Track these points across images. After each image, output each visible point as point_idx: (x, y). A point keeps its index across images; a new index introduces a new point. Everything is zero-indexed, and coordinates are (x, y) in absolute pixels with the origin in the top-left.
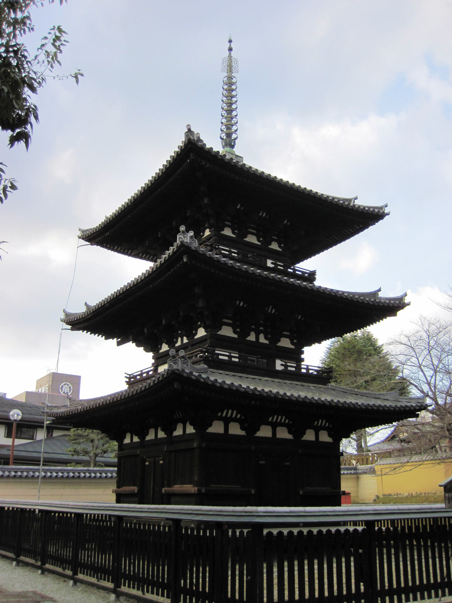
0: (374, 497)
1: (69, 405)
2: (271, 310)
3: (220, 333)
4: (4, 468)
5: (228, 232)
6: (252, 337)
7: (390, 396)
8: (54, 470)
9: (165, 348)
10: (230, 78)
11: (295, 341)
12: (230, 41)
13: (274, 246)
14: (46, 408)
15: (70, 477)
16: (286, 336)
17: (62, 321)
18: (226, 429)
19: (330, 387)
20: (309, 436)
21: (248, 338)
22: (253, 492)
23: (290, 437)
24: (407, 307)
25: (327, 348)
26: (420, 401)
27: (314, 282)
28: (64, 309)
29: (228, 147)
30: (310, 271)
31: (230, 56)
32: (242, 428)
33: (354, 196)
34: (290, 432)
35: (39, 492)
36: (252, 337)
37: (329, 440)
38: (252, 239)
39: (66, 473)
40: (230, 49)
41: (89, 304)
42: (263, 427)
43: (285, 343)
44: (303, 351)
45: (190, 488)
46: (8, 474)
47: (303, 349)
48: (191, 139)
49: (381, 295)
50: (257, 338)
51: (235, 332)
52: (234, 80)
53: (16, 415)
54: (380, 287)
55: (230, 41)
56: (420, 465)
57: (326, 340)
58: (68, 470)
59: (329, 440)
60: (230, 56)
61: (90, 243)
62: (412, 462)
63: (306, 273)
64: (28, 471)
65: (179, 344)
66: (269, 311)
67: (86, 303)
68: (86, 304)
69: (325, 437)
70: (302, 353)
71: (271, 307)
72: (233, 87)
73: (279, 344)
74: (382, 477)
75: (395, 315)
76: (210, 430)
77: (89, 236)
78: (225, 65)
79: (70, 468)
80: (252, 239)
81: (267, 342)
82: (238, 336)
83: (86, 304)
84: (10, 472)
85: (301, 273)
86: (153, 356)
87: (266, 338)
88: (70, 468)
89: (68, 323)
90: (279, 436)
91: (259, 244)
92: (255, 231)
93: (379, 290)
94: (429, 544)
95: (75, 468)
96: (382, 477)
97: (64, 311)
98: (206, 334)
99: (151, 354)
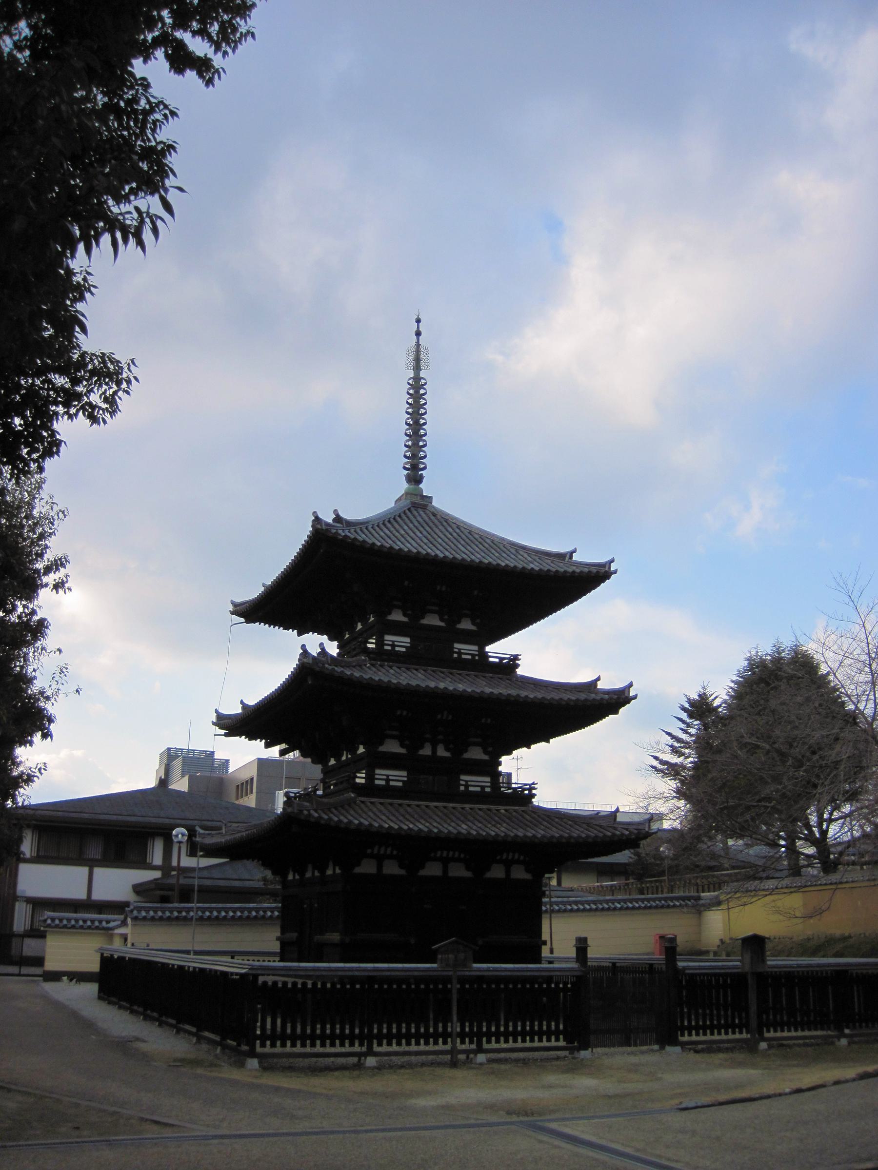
0: (718, 942)
1: (224, 832)
3: (382, 749)
4: (164, 908)
5: (397, 616)
6: (426, 751)
7: (603, 820)
8: (230, 908)
9: (332, 762)
10: (417, 378)
11: (490, 749)
12: (418, 321)
13: (466, 625)
14: (197, 836)
15: (251, 917)
16: (476, 744)
17: (213, 725)
19: (530, 808)
20: (497, 872)
21: (421, 752)
22: (413, 941)
23: (468, 874)
24: (633, 701)
25: (733, 681)
26: (640, 827)
27: (517, 670)
28: (216, 709)
29: (413, 483)
30: (512, 655)
31: (418, 345)
32: (401, 866)
33: (570, 549)
34: (468, 868)
35: (193, 938)
36: (426, 751)
37: (528, 876)
38: (432, 620)
39: (246, 912)
40: (418, 334)
41: (246, 702)
43: (476, 753)
44: (501, 761)
45: (335, 937)
46: (169, 915)
47: (500, 760)
48: (319, 529)
49: (600, 685)
50: (434, 751)
51: (402, 746)
52: (423, 382)
53: (180, 836)
54: (600, 676)
55: (418, 321)
56: (766, 895)
57: (605, 718)
58: (249, 908)
59: (528, 876)
60: (418, 345)
61: (243, 620)
62: (821, 885)
63: (505, 659)
64: (204, 910)
65: (344, 758)
66: (444, 718)
67: (242, 701)
68: (242, 702)
69: (520, 873)
70: (500, 764)
71: (445, 713)
72: (422, 391)
73: (466, 756)
74: (729, 911)
75: (616, 712)
77: (243, 612)
78: (411, 358)
79: (252, 905)
80: (432, 620)
81: (447, 754)
82: (407, 751)
83: (242, 702)
84: (171, 912)
85: (497, 660)
86: (322, 770)
87: (447, 749)
88: (266, 905)
89: (221, 728)
90: (451, 874)
91: (442, 624)
92: (437, 608)
93: (598, 679)
94: (685, 1010)
95: (259, 905)
96: (729, 911)
97: (216, 711)
98: (364, 750)
99: (319, 767)
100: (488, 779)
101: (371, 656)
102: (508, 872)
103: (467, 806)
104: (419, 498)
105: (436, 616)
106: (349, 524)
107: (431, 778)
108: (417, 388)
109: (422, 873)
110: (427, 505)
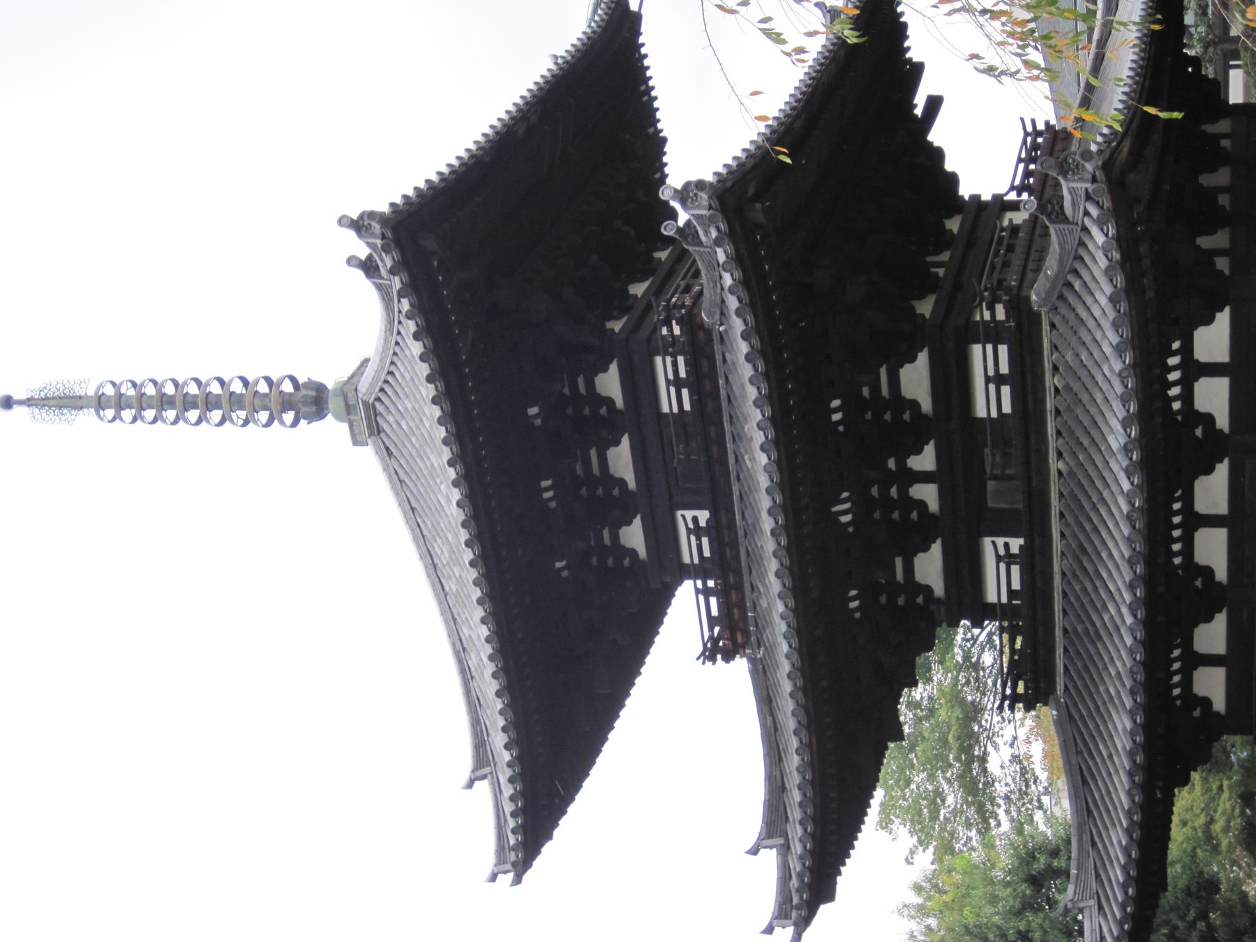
2: (844, 514)
5: (634, 536)
10: (100, 402)
18: (1212, 660)
21: (933, 506)
31: (29, 402)
36: (928, 494)
42: (1201, 557)
50: (925, 477)
60: (29, 402)
76: (1219, 705)
87: (919, 451)
90: (1222, 508)
100: (977, 349)
101: (740, 640)
102: (1213, 370)
103: (1055, 465)
104: (353, 417)
105: (612, 453)
106: (482, 758)
107: (991, 485)
108: (120, 403)
109: (1221, 574)
110: (365, 403)
